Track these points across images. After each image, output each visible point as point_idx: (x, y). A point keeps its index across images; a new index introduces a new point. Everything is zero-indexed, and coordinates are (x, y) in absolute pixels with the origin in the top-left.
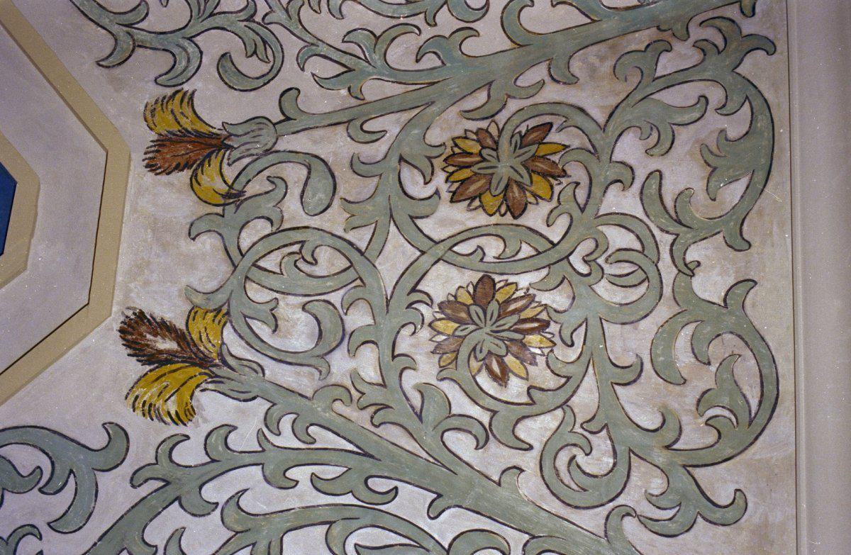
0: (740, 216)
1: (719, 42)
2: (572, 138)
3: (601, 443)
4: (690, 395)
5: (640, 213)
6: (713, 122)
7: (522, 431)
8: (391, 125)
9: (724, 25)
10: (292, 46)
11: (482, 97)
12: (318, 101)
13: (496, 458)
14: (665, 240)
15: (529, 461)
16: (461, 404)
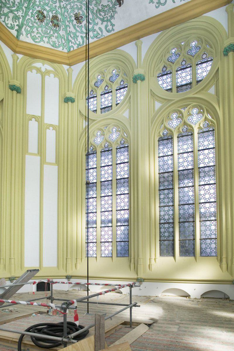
0: (50, 43)
1: (64, 45)
2: (57, 29)
3: (32, 25)
4: (36, 35)
5: (51, 34)
6: (57, 43)
7: (32, 17)
8: (60, 11)
9: (65, 46)
10: (67, 3)
11: (62, 21)
12: (62, 4)
13: (30, 14)
14: (48, 36)
15: (30, 17)
16: (35, 12)
